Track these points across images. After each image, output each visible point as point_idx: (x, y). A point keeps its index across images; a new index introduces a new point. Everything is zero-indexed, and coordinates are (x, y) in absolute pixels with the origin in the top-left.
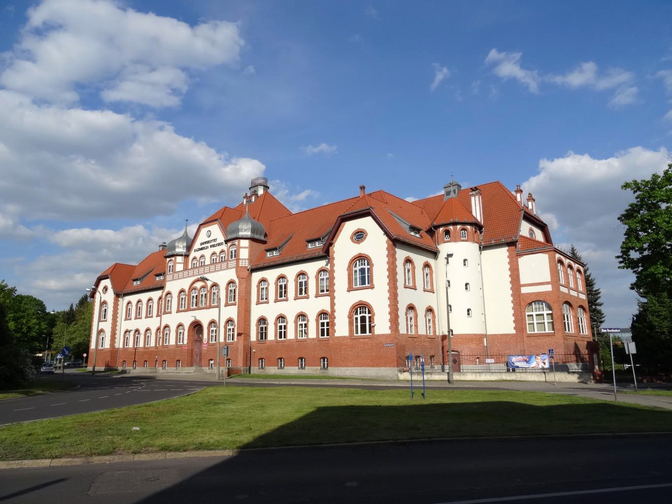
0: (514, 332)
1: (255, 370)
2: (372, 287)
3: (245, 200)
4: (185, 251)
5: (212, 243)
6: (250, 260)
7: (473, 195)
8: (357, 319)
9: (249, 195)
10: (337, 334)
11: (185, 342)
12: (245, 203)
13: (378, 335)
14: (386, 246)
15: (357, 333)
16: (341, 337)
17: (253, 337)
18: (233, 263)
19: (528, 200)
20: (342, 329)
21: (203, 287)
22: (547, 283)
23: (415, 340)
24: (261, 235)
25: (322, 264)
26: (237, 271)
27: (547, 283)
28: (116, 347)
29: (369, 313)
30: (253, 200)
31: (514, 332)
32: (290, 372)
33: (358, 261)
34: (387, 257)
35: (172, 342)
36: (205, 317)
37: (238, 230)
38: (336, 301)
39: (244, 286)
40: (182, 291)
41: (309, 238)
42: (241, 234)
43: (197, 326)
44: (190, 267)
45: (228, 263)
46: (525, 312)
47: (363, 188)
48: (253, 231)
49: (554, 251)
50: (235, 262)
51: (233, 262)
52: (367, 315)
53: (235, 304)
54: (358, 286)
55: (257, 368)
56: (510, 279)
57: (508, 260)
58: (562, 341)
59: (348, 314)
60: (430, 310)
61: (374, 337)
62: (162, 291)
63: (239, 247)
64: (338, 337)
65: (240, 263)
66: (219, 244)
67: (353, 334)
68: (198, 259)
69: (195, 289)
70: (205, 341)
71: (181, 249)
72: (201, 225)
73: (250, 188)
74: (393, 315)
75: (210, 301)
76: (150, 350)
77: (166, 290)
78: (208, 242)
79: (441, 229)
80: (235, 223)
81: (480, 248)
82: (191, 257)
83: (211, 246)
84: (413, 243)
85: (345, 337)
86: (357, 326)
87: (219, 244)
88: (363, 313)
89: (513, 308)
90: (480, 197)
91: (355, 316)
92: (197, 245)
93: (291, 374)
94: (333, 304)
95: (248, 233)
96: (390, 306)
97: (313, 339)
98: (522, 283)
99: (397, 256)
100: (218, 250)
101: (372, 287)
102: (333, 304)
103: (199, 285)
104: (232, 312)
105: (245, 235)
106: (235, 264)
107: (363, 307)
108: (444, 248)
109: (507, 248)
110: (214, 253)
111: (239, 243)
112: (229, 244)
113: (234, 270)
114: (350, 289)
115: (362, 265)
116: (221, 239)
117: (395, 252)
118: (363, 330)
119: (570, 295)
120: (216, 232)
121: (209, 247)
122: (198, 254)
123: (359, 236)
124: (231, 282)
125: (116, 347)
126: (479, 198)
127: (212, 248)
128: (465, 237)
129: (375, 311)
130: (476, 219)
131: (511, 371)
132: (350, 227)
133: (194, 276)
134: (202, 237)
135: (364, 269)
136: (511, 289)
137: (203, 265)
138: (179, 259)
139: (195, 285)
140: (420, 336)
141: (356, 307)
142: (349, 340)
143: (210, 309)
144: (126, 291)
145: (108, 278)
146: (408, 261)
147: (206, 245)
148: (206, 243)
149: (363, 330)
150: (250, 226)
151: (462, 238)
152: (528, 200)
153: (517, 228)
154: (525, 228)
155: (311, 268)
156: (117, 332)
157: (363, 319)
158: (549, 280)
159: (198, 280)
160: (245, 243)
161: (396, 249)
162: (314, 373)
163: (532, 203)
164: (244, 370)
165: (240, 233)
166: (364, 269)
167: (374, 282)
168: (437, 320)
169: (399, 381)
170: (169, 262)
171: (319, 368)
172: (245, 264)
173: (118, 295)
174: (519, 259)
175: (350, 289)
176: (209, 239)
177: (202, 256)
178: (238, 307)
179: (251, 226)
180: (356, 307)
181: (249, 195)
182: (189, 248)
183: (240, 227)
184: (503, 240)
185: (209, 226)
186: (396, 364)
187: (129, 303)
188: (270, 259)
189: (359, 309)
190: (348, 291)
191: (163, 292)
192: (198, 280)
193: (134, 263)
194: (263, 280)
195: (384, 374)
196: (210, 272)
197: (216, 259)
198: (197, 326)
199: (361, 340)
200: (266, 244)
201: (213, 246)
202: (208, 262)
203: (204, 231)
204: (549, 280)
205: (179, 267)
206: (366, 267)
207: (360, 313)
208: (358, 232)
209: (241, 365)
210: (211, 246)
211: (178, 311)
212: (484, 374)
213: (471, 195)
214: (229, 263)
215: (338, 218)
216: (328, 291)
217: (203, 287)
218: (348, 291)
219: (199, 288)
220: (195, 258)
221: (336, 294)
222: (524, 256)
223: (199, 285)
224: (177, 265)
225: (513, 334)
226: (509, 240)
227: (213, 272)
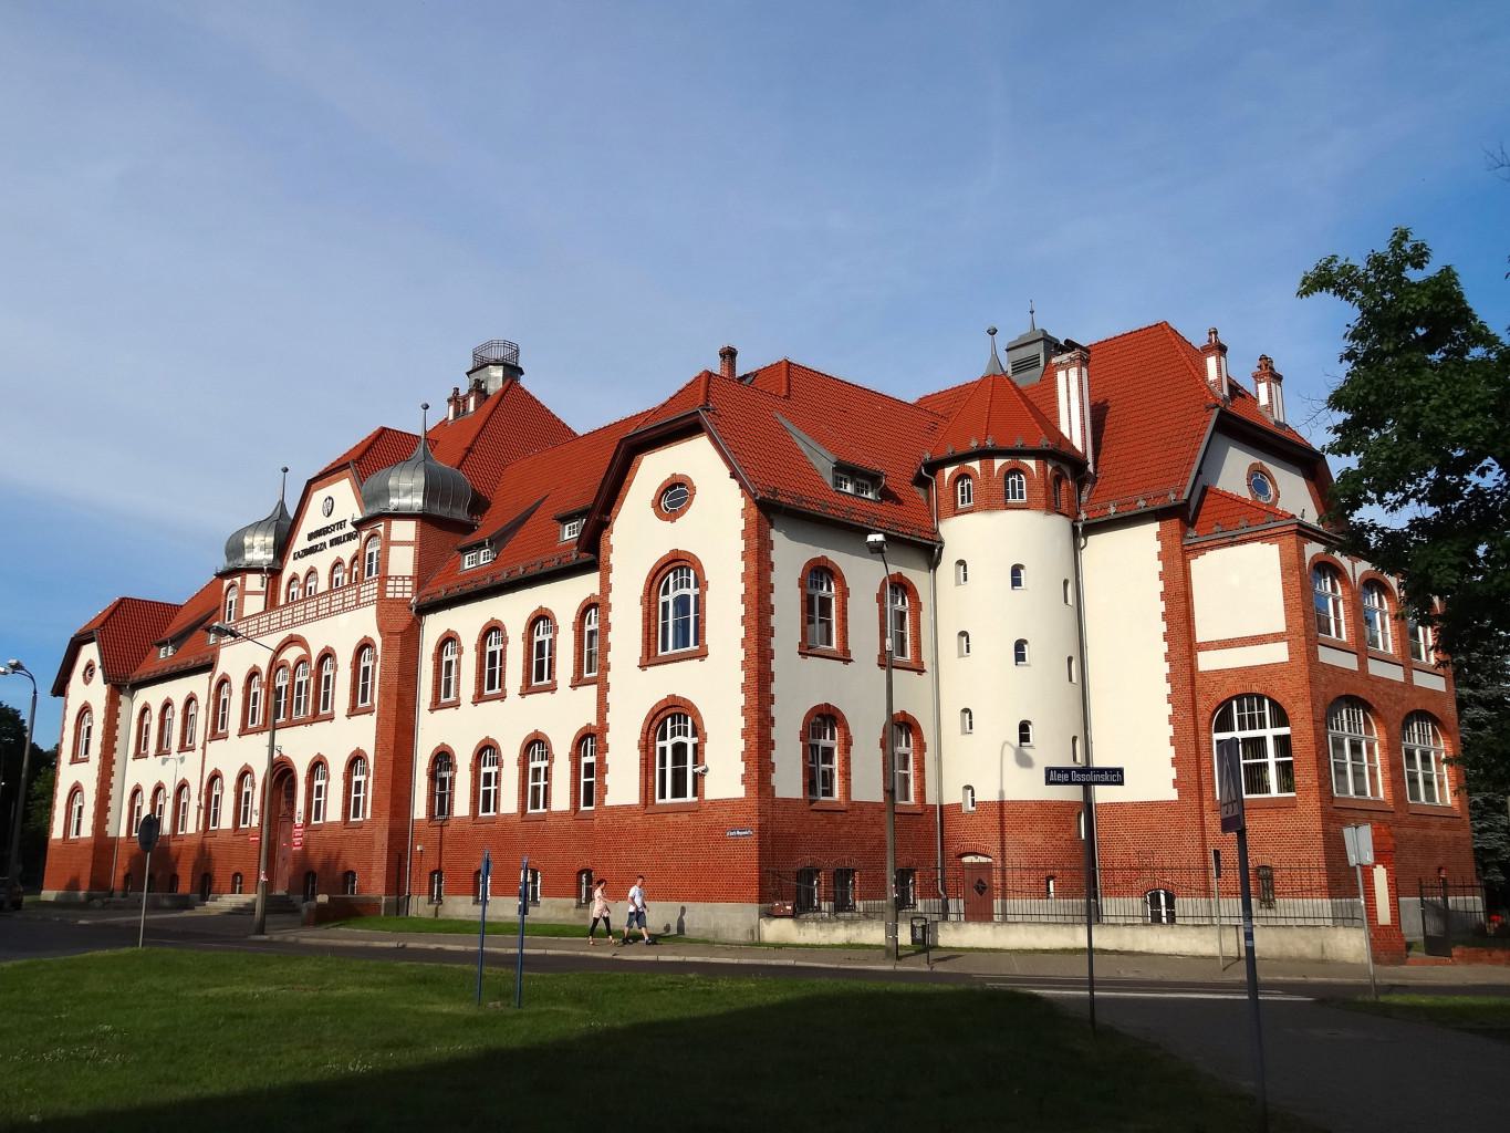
0: (1173, 795)
1: (419, 906)
2: (702, 655)
3: (452, 408)
4: (271, 557)
6: (421, 577)
7: (1061, 366)
8: (663, 750)
9: (462, 393)
10: (610, 800)
12: (451, 418)
13: (714, 803)
14: (741, 524)
15: (663, 796)
16: (619, 808)
17: (420, 810)
18: (370, 590)
19: (1257, 378)
20: (623, 786)
21: (302, 662)
22: (1276, 638)
23: (838, 817)
24: (456, 505)
25: (587, 585)
26: (379, 614)
27: (1276, 638)
28: (109, 835)
29: (695, 734)
30: (472, 409)
31: (1173, 795)
32: (501, 914)
33: (671, 575)
34: (743, 558)
36: (299, 745)
37: (386, 493)
38: (610, 697)
39: (396, 655)
40: (253, 673)
41: (562, 512)
42: (395, 502)
43: (281, 773)
44: (282, 602)
45: (359, 592)
46: (1210, 732)
47: (729, 355)
48: (430, 492)
49: (1299, 533)
50: (376, 585)
52: (690, 741)
53: (369, 711)
54: (671, 650)
55: (425, 898)
56: (1163, 627)
57: (1159, 566)
58: (1318, 826)
59: (638, 736)
60: (903, 725)
61: (702, 808)
62: (209, 674)
63: (388, 543)
64: (612, 808)
65: (389, 589)
67: (654, 801)
68: (302, 581)
71: (259, 550)
72: (310, 483)
73: (468, 374)
74: (754, 739)
75: (316, 702)
76: (184, 844)
77: (220, 670)
79: (949, 471)
80: (382, 471)
81: (1075, 529)
84: (830, 513)
85: (629, 807)
86: (663, 773)
88: (679, 734)
89: (1172, 720)
90: (1084, 370)
91: (659, 744)
92: (300, 542)
93: (506, 917)
94: (603, 707)
95: (416, 502)
96: (745, 711)
97: (562, 814)
98: (1201, 637)
99: (775, 556)
100: (347, 551)
101: (702, 655)
102: (603, 707)
103: (291, 655)
104: (362, 733)
105: (406, 507)
106: (376, 591)
107: (679, 715)
108: (963, 533)
109: (1155, 527)
110: (338, 563)
111: (388, 530)
112: (365, 534)
113: (373, 608)
114: (649, 659)
115: (682, 587)
117: (770, 545)
118: (679, 790)
119: (1369, 678)
120: (344, 499)
123: (675, 496)
124: (365, 645)
125: (109, 835)
126: (1080, 373)
128: (1021, 497)
129: (708, 727)
130: (1069, 443)
131: (1164, 920)
132: (653, 470)
133: (282, 628)
134: (313, 519)
135: (688, 596)
136: (1168, 657)
137: (310, 595)
138: (254, 582)
139: (283, 656)
140: (862, 806)
141: (662, 716)
142: (638, 818)
143: (314, 725)
144: (136, 676)
145: (92, 640)
146: (819, 572)
149: (679, 790)
150: (420, 481)
151: (1010, 500)
152: (1257, 378)
153: (1210, 463)
154: (1235, 470)
155: (564, 598)
156: (111, 792)
157: (679, 749)
158: (1281, 627)
159: (292, 641)
160: (405, 530)
161: (773, 531)
162: (561, 916)
163: (1269, 387)
164: (386, 904)
165: (392, 500)
166: (688, 596)
167: (711, 638)
168: (929, 756)
169: (757, 944)
170: (228, 590)
171: (574, 901)
172: (403, 590)
173: (121, 684)
174: (1194, 563)
175: (649, 659)
176: (333, 519)
177: (312, 572)
178: (378, 718)
179: (423, 480)
180: (662, 716)
181: (462, 393)
182: (281, 548)
183: (391, 483)
184: (1142, 503)
185: (330, 483)
186: (755, 890)
187: (145, 709)
188: (470, 573)
189: (669, 720)
190: (642, 667)
191: (211, 678)
193: (181, 600)
194: (449, 639)
195: (723, 924)
197: (343, 578)
198: (281, 773)
199: (670, 818)
200: (473, 534)
202: (323, 586)
203: (318, 498)
204: (1281, 627)
205: (254, 604)
206: (692, 592)
207: (673, 735)
208: (673, 486)
209: (381, 890)
211: (244, 731)
212: (1020, 927)
213: (1056, 365)
214: (362, 589)
215: (619, 446)
216: (592, 665)
217: (301, 661)
218: (642, 667)
219: (292, 664)
220: (294, 578)
221: (611, 677)
222: (1209, 553)
223: (291, 655)
224: (247, 598)
225: (1169, 803)
226: (1158, 504)
227: (325, 616)
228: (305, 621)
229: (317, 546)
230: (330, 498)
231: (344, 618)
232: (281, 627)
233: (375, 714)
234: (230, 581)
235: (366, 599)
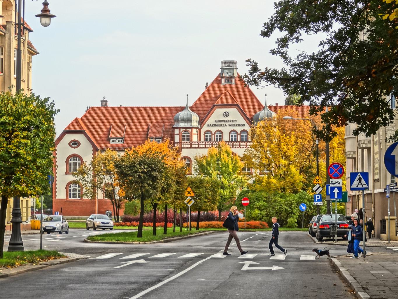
5: (231, 123)
66: (240, 125)
78: (226, 121)
82: (203, 130)
83: (230, 125)
87: (240, 125)
92: (211, 120)
100: (239, 129)
116: (241, 120)
147: (225, 123)
148: (222, 121)
201: (233, 125)
220: (208, 131)
229: (221, 125)
230: (227, 112)
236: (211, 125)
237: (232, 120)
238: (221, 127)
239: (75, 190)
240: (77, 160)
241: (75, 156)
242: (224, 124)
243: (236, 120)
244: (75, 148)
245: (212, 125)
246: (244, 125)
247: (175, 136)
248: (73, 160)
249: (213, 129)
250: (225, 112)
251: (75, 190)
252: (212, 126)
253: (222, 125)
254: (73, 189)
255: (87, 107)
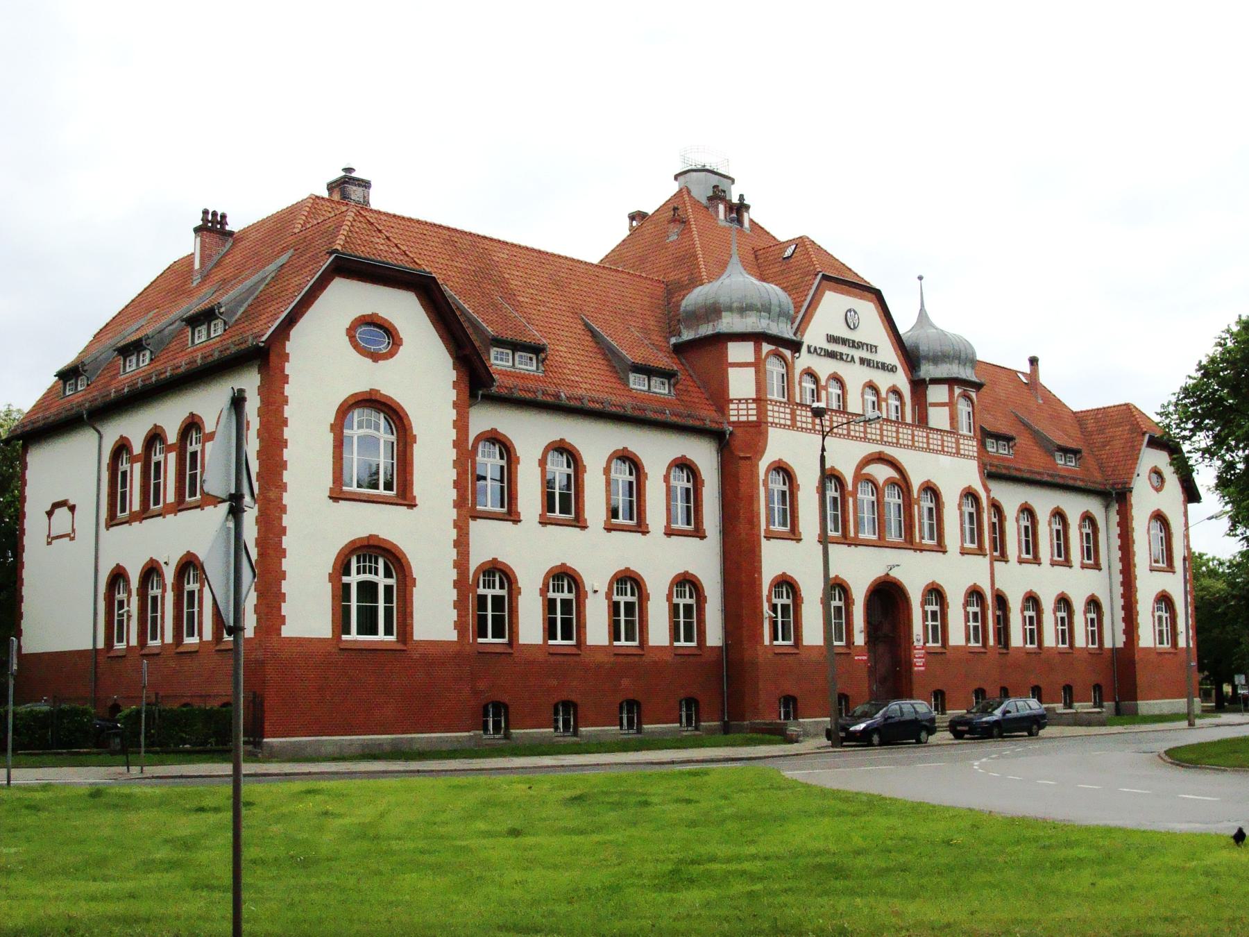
11: (859, 639)
35: (813, 632)
51: (970, 443)
66: (884, 367)
69: (870, 480)
70: (918, 641)
83: (862, 361)
103: (882, 473)
121: (857, 360)
122: (824, 368)
127: (865, 368)
139: (867, 470)
148: (844, 342)
159: (880, 458)
192: (880, 458)
196: (913, 447)
210: (862, 361)
228: (897, 444)
229: (841, 354)
230: (855, 313)
231: (943, 459)
232: (865, 438)
233: (988, 556)
234: (773, 347)
235: (967, 453)
236: (815, 349)
237: (867, 345)
238: (842, 362)
239: (368, 590)
240: (377, 428)
241: (373, 402)
242: (848, 355)
243: (876, 347)
244: (376, 357)
245: (819, 351)
246: (892, 369)
247: (731, 370)
248: (360, 426)
249: (824, 368)
250: (850, 310)
251: (368, 590)
252: (820, 355)
253: (844, 357)
254: (361, 585)
255: (206, 212)
